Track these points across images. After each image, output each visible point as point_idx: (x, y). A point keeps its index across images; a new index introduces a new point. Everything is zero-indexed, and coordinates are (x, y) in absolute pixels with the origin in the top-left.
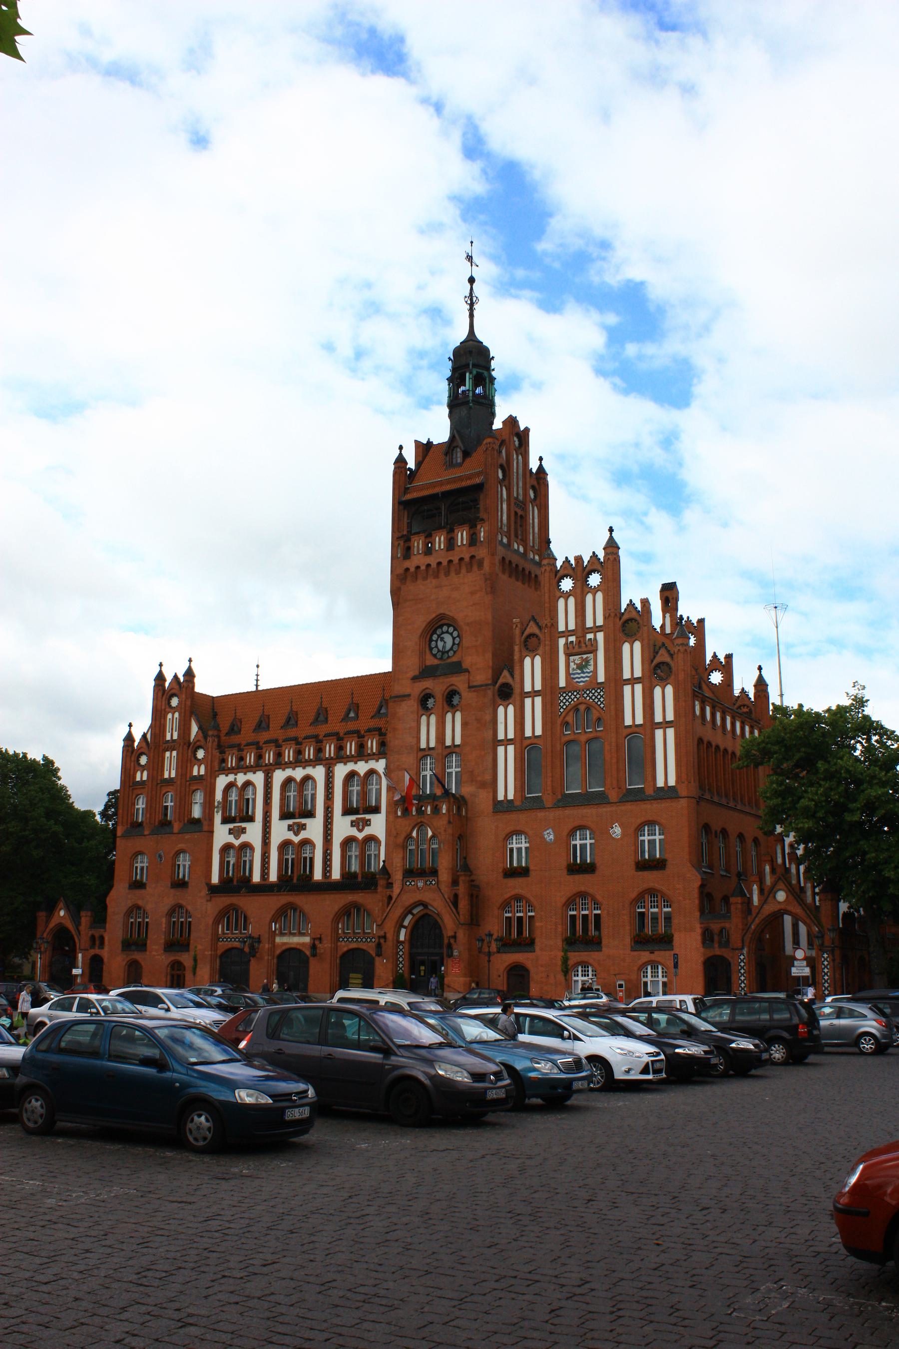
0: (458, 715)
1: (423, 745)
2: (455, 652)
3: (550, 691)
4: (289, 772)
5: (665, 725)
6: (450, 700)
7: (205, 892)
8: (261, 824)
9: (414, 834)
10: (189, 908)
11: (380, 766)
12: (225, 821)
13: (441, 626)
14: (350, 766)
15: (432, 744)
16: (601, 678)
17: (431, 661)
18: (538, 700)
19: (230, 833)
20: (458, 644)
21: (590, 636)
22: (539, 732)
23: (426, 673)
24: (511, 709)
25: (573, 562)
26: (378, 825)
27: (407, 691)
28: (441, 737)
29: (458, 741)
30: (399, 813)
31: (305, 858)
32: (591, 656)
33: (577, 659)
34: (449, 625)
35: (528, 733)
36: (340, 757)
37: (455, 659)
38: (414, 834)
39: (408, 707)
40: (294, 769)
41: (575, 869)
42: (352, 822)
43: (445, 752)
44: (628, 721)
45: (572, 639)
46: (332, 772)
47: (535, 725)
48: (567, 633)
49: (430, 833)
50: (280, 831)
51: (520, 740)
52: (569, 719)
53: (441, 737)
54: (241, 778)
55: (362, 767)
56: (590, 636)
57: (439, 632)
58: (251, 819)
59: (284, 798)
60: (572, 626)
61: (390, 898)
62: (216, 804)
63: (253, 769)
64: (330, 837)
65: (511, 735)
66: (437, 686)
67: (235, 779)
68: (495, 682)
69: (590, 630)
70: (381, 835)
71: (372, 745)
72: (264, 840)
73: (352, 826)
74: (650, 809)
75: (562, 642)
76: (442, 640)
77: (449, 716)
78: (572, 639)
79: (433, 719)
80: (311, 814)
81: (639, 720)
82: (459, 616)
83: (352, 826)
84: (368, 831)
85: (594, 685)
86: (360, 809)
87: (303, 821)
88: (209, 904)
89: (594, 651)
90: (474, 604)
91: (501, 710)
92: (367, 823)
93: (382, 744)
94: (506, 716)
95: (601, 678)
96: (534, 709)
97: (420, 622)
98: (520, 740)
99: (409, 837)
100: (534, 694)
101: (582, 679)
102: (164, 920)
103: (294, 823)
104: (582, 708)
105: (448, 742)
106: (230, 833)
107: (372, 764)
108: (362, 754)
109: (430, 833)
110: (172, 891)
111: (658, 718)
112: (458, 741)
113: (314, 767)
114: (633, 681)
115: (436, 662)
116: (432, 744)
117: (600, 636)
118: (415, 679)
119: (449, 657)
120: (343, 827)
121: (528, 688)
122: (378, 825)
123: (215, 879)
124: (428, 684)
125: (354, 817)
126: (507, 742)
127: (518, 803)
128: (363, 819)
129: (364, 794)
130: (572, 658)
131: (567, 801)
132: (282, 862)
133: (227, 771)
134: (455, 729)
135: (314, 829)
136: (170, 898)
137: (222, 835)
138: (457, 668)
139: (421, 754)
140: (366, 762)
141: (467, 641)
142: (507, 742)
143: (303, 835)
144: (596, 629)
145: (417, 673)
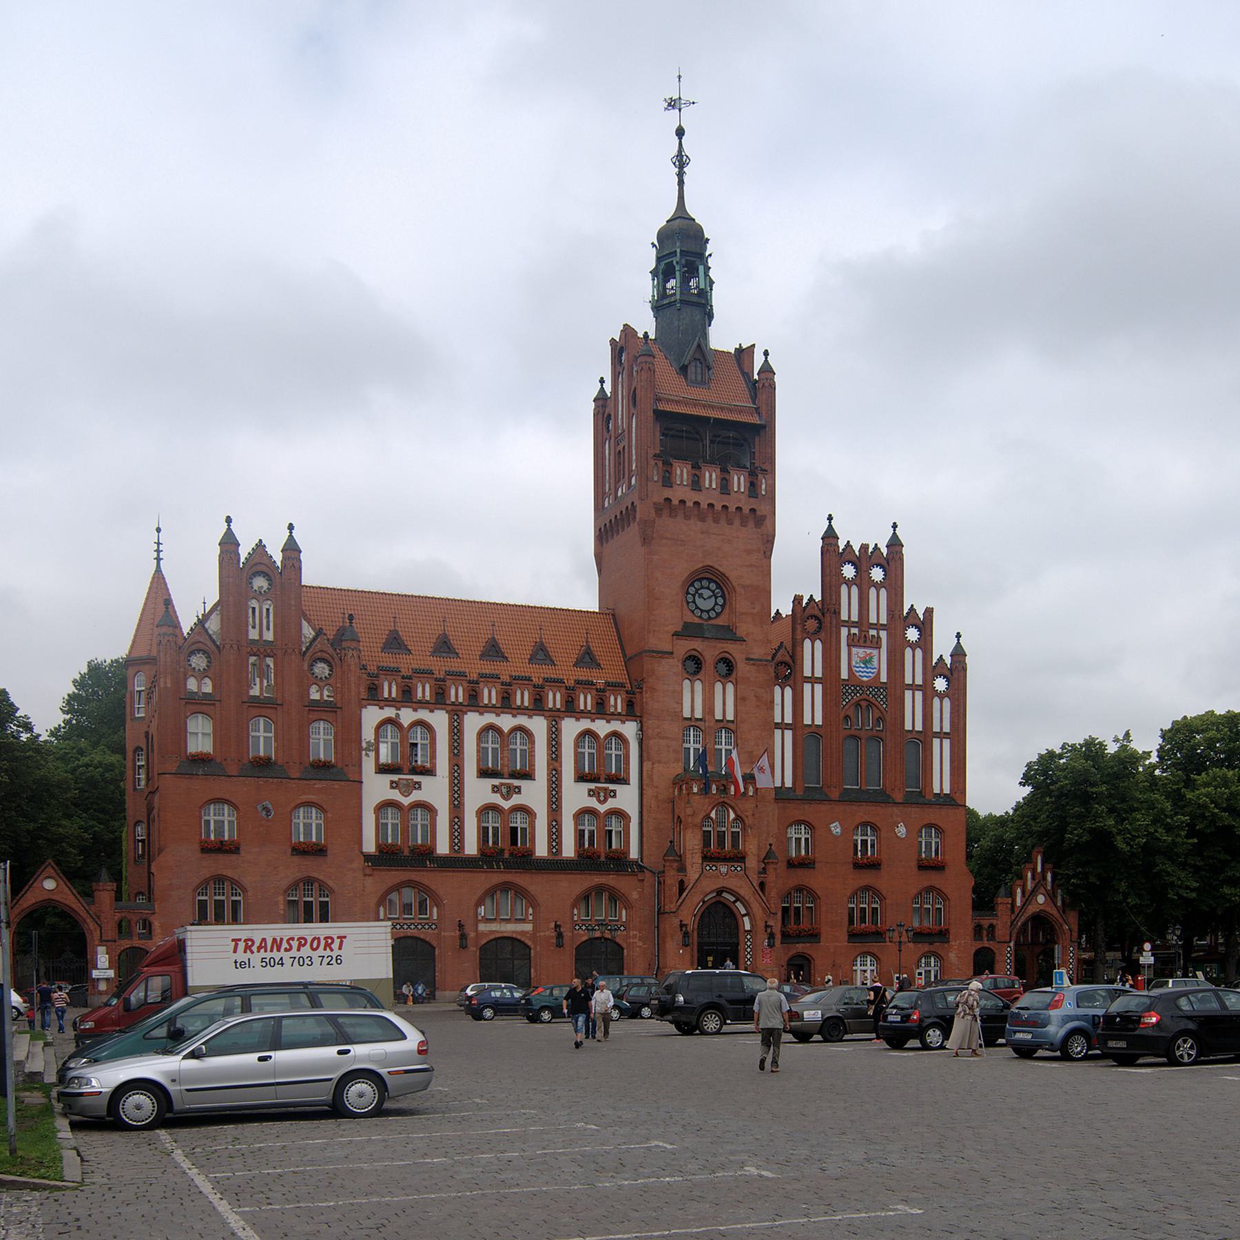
0: (730, 688)
1: (687, 714)
2: (718, 615)
3: (830, 678)
4: (490, 718)
5: (942, 735)
6: (727, 667)
7: (359, 863)
8: (447, 780)
9: (713, 815)
10: (330, 883)
11: (629, 729)
12: (382, 769)
13: (700, 580)
14: (585, 724)
15: (698, 715)
16: (884, 679)
17: (690, 618)
18: (818, 688)
19: (392, 787)
20: (723, 606)
21: (873, 632)
22: (818, 721)
23: (688, 631)
24: (788, 691)
25: (856, 549)
26: (627, 798)
27: (668, 648)
28: (709, 707)
29: (730, 717)
30: (695, 790)
31: (514, 830)
32: (875, 652)
33: (859, 652)
34: (710, 580)
35: (807, 721)
36: (570, 708)
37: (719, 621)
38: (713, 815)
39: (670, 668)
40: (498, 715)
41: (924, 866)
42: (590, 790)
43: (707, 726)
44: (908, 727)
45: (855, 631)
46: (461, 724)
47: (814, 713)
48: (849, 624)
49: (732, 816)
50: (478, 792)
51: (796, 725)
52: (851, 713)
53: (709, 707)
54: (407, 716)
55: (602, 728)
56: (873, 632)
57: (697, 585)
58: (430, 772)
59: (578, 758)
60: (855, 618)
61: (682, 887)
62: (364, 745)
63: (430, 706)
64: (556, 807)
65: (788, 719)
66: (710, 651)
67: (398, 715)
68: (773, 658)
69: (872, 626)
70: (632, 810)
71: (617, 703)
72: (454, 803)
73: (590, 795)
74: (933, 815)
75: (844, 632)
76: (701, 596)
77: (718, 687)
78: (855, 631)
79: (698, 686)
80: (528, 775)
81: (919, 727)
82: (733, 575)
83: (590, 795)
84: (611, 804)
85: (875, 683)
86: (599, 776)
87: (516, 782)
88: (369, 880)
89: (878, 647)
90: (751, 565)
91: (777, 689)
92: (613, 794)
93: (630, 704)
94: (783, 698)
95: (884, 679)
96: (814, 697)
97: (683, 569)
98: (796, 725)
99: (708, 817)
100: (812, 680)
101: (865, 676)
102: (281, 899)
103: (502, 784)
104: (864, 704)
105: (718, 716)
106: (392, 787)
107: (616, 726)
108: (601, 710)
109: (732, 816)
110: (296, 859)
111: (936, 728)
112: (730, 717)
113: (530, 717)
114: (913, 687)
115: (697, 620)
116: (698, 715)
117: (883, 634)
118: (675, 634)
119: (710, 618)
120: (576, 796)
121: (807, 672)
122: (627, 798)
123: (370, 846)
124: (697, 645)
125: (592, 786)
126: (782, 726)
127: (799, 793)
128: (606, 789)
129: (603, 759)
130: (854, 650)
131: (850, 798)
132: (483, 832)
133: (384, 703)
134: (725, 702)
135: (534, 794)
136: (296, 868)
137: (376, 788)
138: (728, 634)
139: (688, 723)
140: (608, 722)
141: (741, 604)
142: (782, 726)
143: (516, 800)
144: (878, 626)
145: (679, 628)
